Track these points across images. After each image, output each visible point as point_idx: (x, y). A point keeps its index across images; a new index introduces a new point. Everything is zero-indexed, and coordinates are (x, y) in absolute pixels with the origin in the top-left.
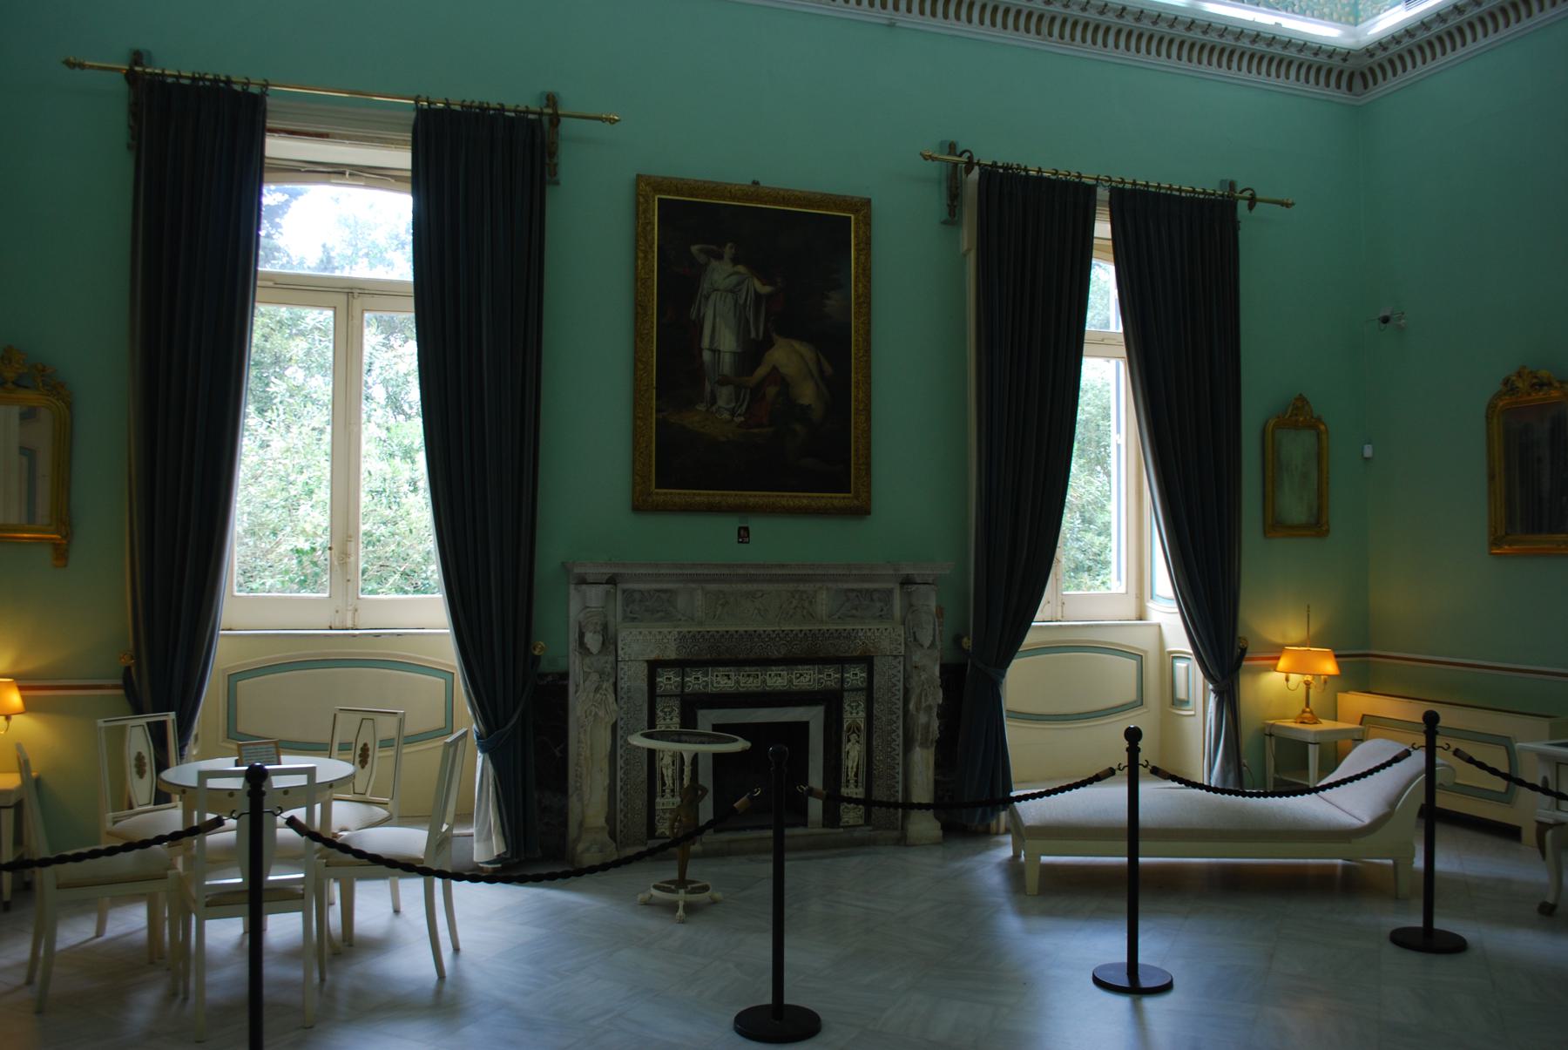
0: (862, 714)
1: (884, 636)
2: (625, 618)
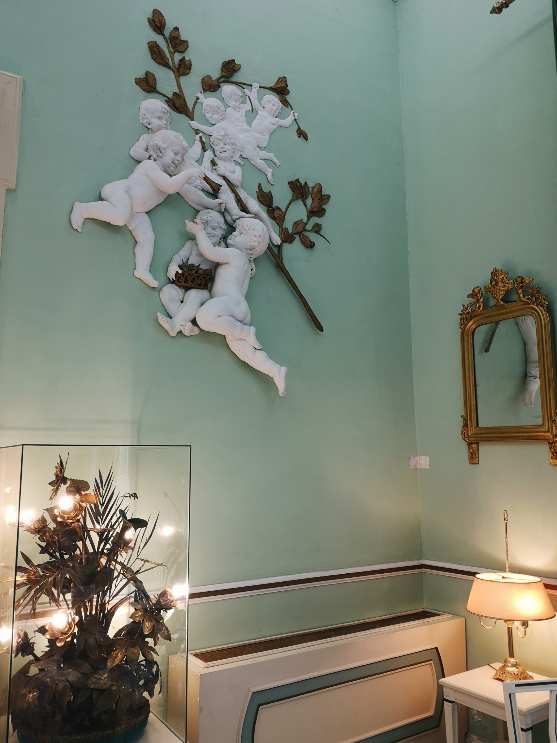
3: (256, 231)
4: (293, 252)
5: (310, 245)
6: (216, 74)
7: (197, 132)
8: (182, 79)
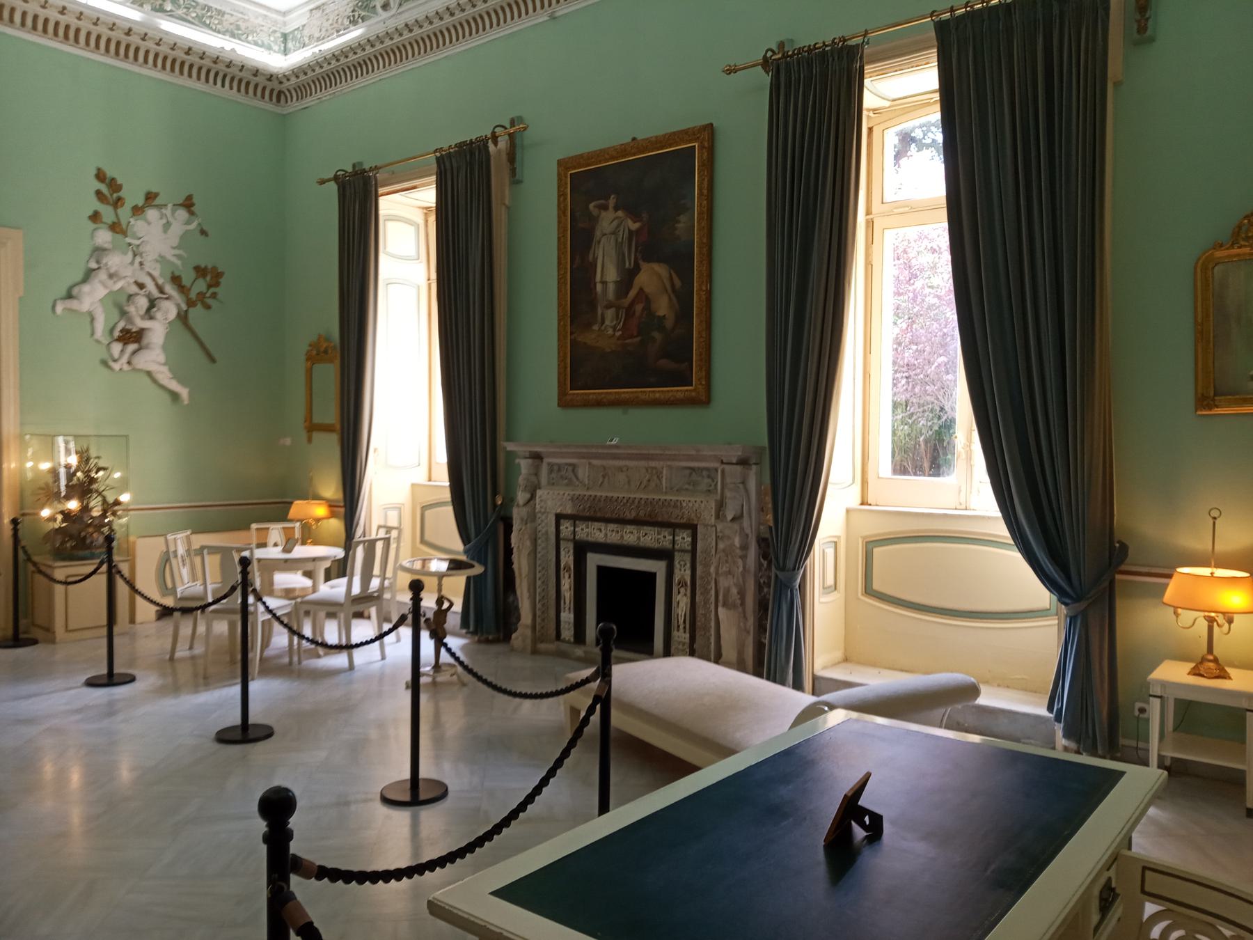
0: (688, 572)
1: (701, 506)
2: (549, 483)
3: (169, 310)
4: (196, 313)
5: (208, 307)
6: (141, 202)
7: (130, 244)
8: (119, 211)
